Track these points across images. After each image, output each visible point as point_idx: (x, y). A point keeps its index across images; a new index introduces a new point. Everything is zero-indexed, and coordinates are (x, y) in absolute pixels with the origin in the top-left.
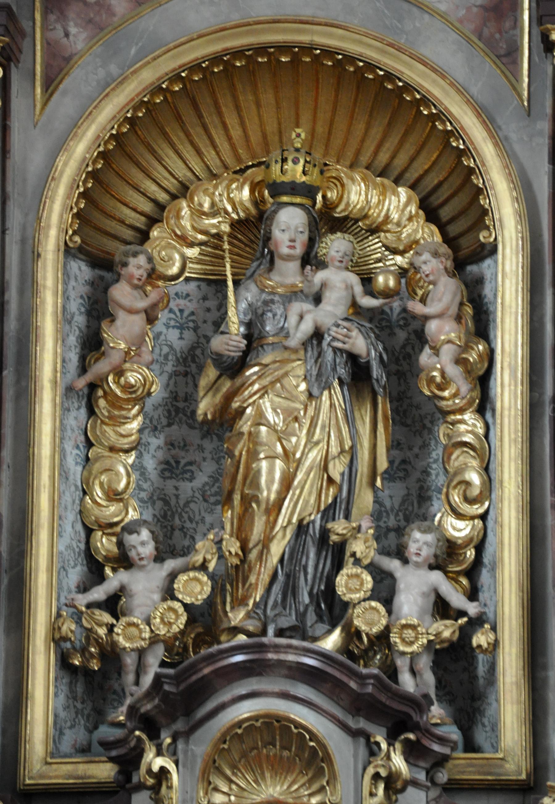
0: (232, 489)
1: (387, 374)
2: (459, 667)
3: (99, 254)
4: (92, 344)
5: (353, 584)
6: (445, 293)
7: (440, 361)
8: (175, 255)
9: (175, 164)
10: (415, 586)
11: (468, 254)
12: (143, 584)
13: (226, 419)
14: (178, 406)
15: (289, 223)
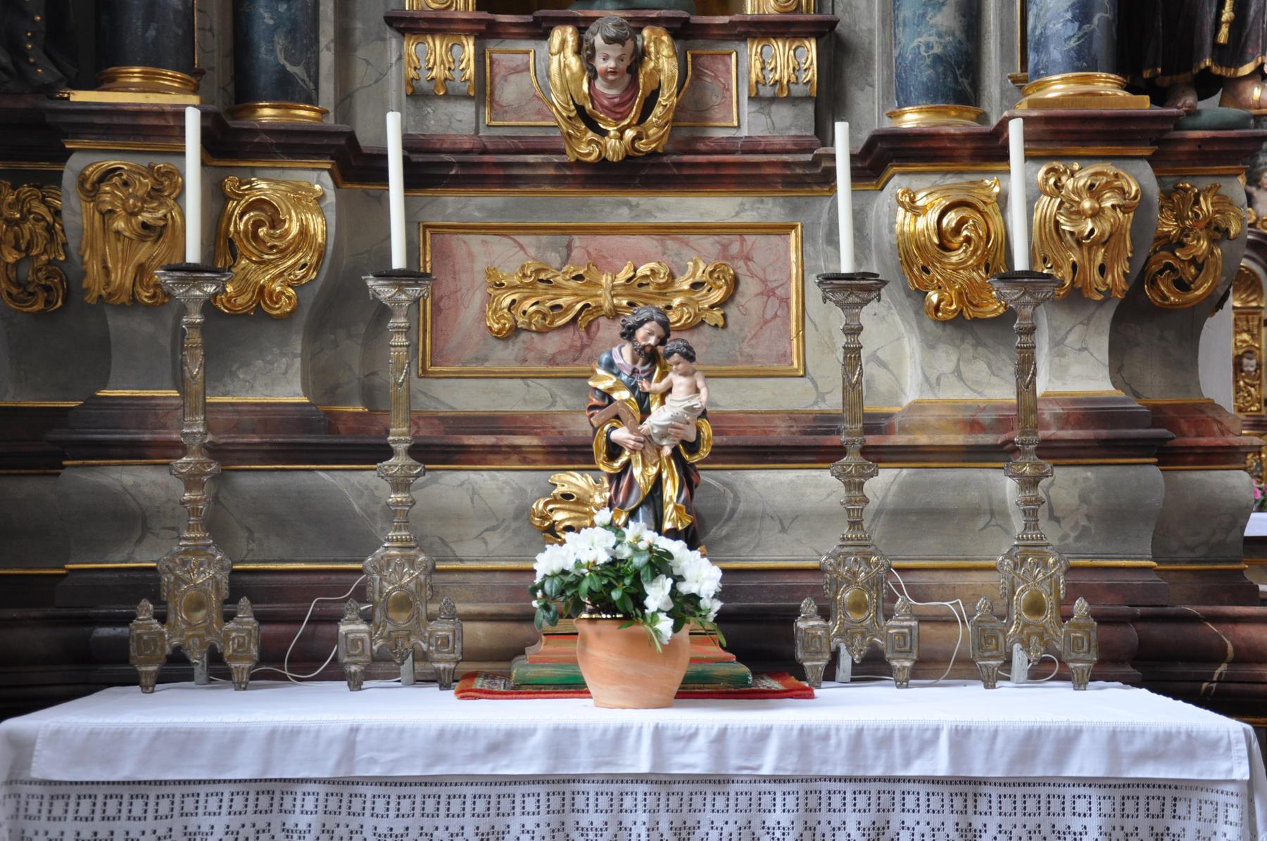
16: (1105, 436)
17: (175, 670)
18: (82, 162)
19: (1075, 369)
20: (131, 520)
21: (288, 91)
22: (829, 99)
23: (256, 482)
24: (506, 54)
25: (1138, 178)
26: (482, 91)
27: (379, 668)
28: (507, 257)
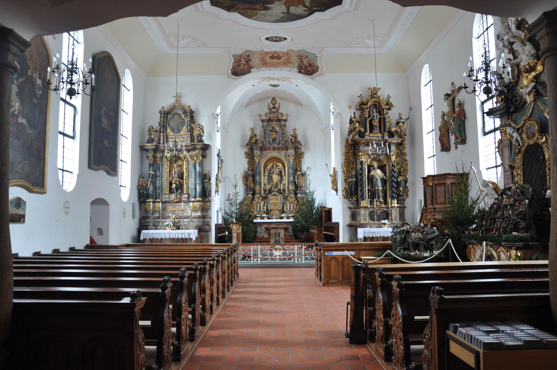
0: (272, 180)
1: (280, 174)
2: (284, 190)
3: (265, 167)
4: (264, 173)
5: (278, 186)
6: (283, 170)
7: (283, 174)
8: (269, 168)
9: (269, 162)
10: (282, 186)
11: (284, 167)
12: (267, 186)
13: (272, 177)
14: (269, 176)
15: (275, 166)
16: (199, 217)
17: (151, 229)
18: (147, 204)
19: (199, 214)
20: (149, 222)
21: (158, 198)
22: (188, 197)
23: (156, 220)
24: (171, 196)
25: (201, 203)
26: (169, 198)
27: (160, 229)
28: (170, 207)
